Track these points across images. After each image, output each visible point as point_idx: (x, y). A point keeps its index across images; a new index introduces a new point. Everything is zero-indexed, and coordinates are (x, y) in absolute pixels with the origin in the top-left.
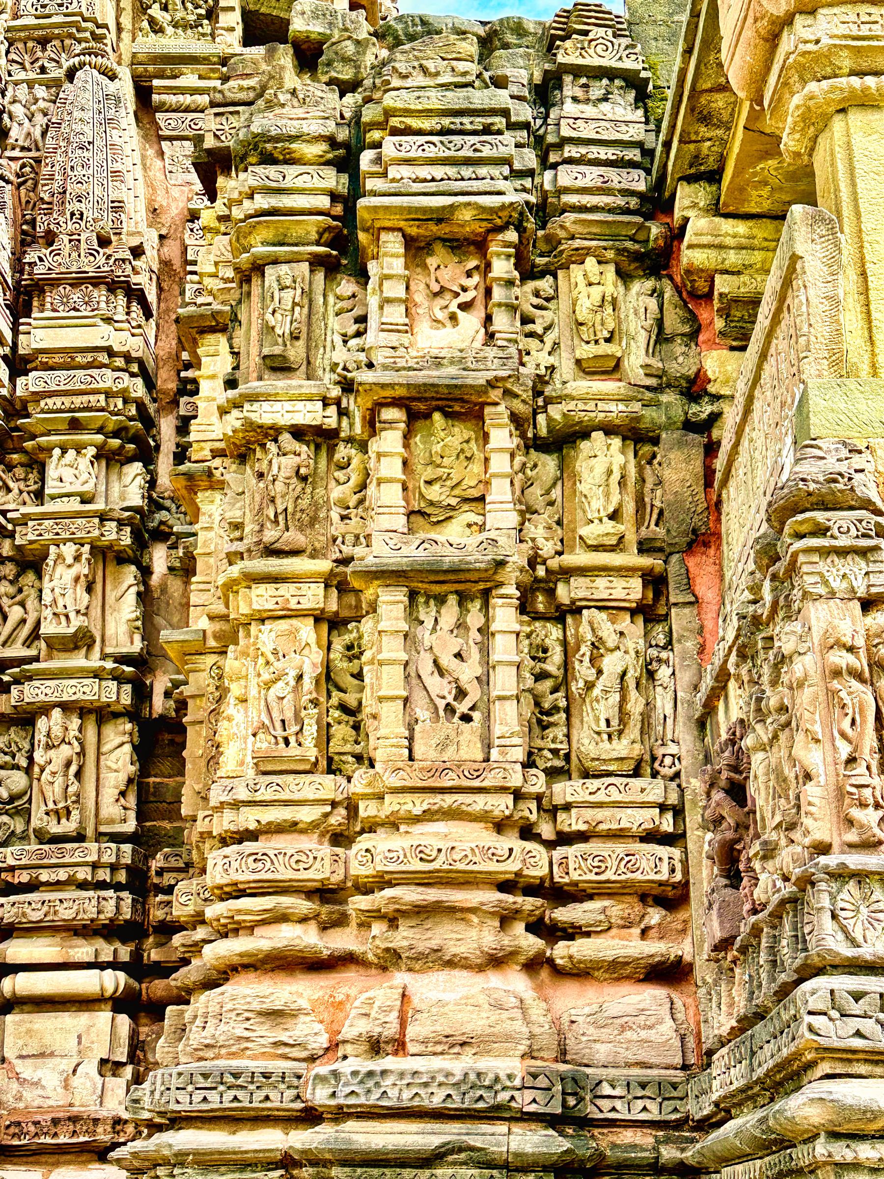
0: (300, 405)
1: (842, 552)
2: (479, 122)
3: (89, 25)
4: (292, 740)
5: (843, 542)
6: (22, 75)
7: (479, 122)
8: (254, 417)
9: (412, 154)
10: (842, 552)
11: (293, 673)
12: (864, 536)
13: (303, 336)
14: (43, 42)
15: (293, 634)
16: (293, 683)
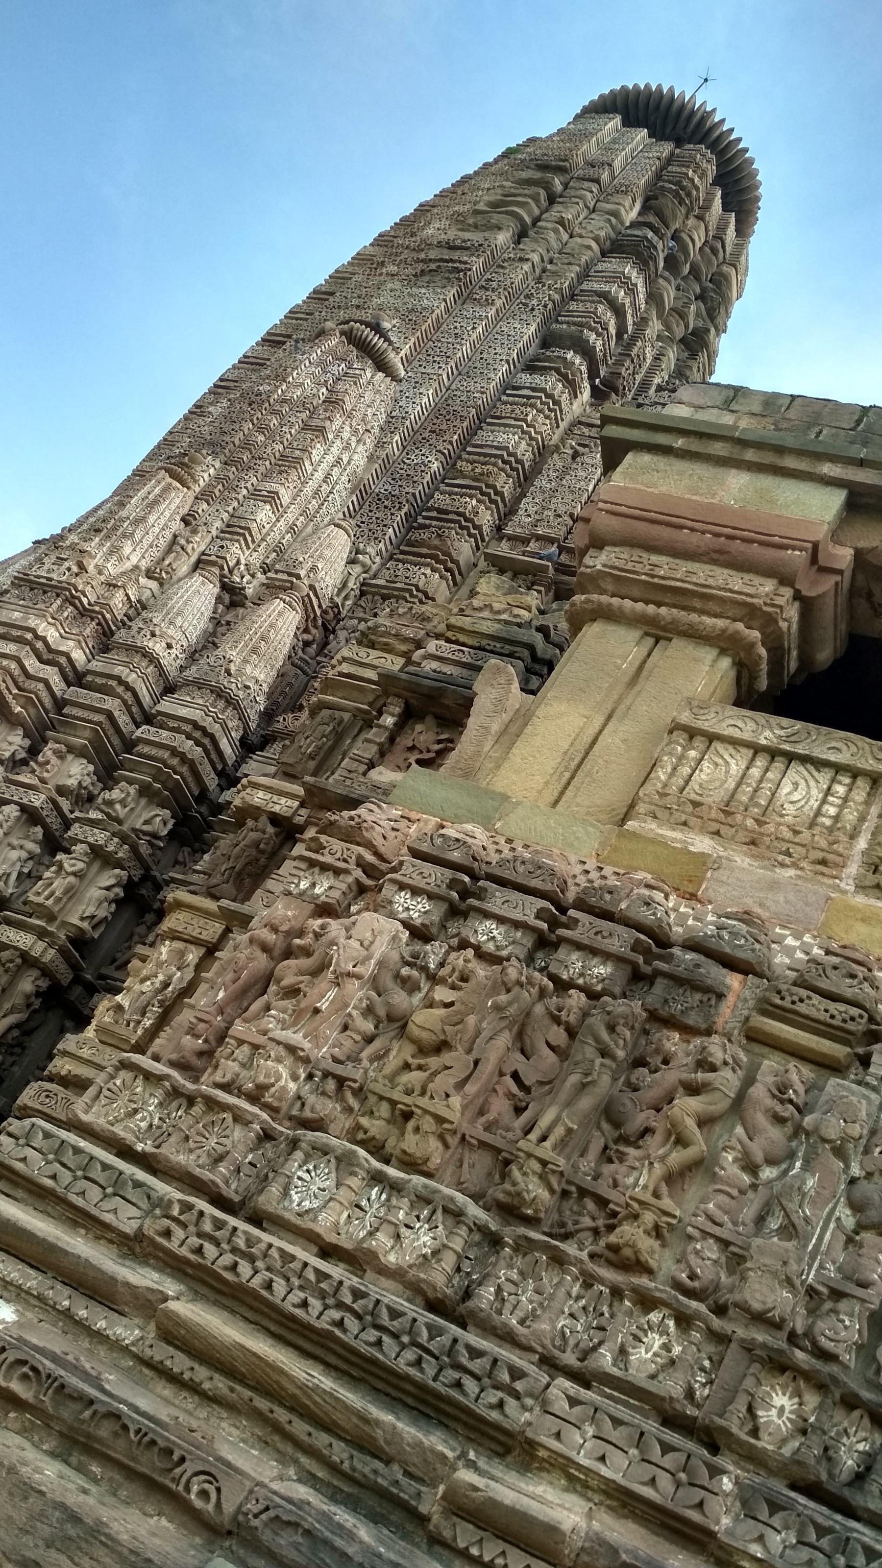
0: (283, 801)
1: (324, 868)
2: (508, 648)
3: (420, 595)
4: (132, 1024)
5: (327, 859)
6: (361, 615)
7: (508, 648)
8: (248, 798)
9: (444, 655)
10: (324, 868)
11: (161, 977)
12: (345, 861)
13: (318, 758)
14: (385, 598)
15: (182, 954)
16: (157, 985)
